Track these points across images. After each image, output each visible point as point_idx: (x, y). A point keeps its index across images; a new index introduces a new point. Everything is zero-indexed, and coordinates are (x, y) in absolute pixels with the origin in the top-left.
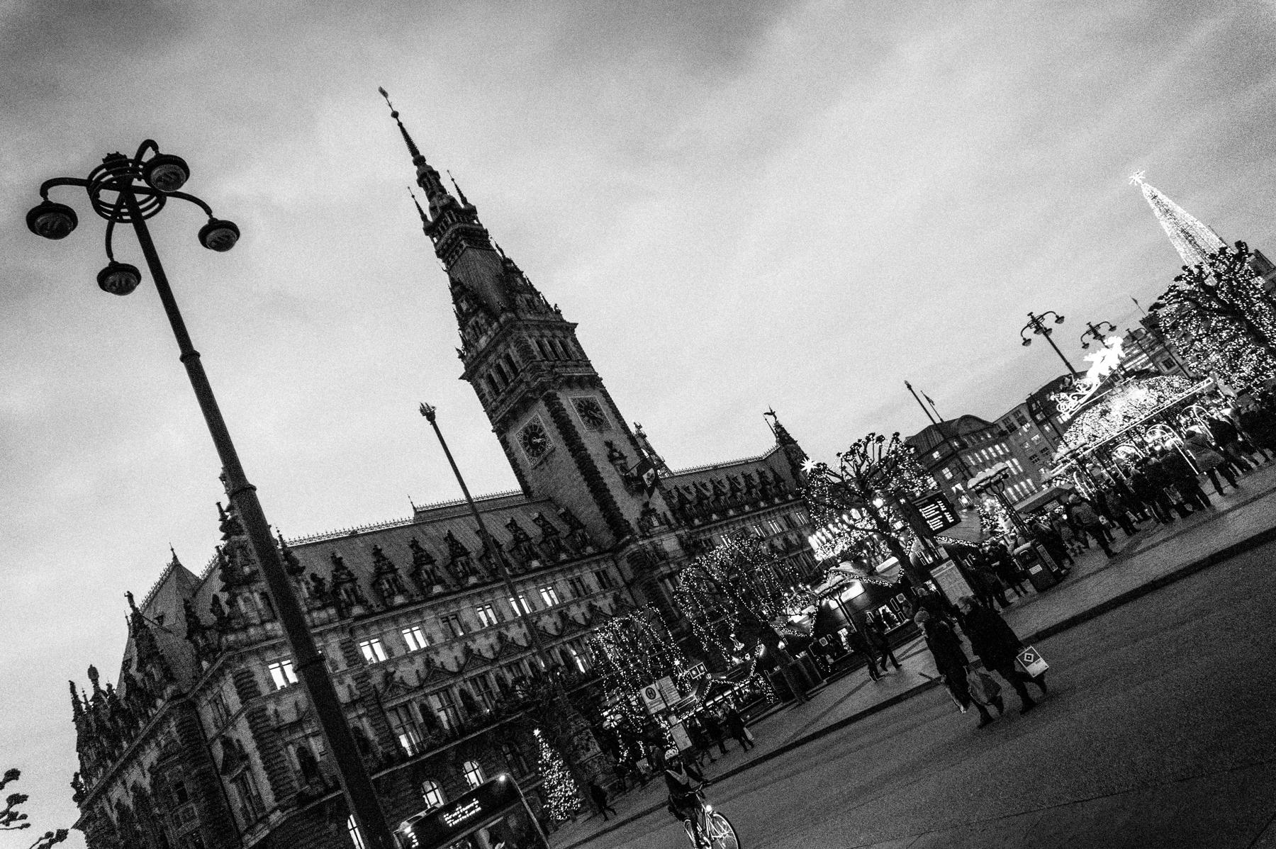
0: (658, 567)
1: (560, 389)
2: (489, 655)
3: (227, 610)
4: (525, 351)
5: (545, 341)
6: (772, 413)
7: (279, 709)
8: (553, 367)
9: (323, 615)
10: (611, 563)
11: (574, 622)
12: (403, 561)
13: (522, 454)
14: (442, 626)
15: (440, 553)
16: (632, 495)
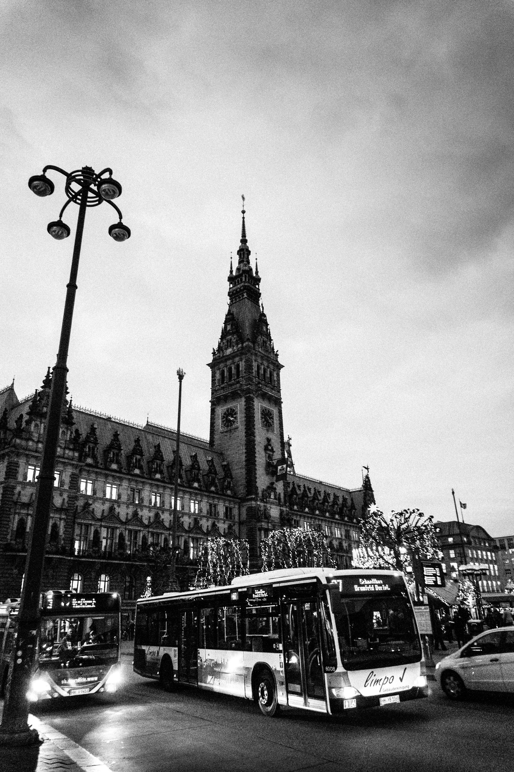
0: (262, 522)
1: (257, 397)
2: (146, 522)
3: (24, 425)
4: (249, 367)
5: (262, 367)
6: (367, 469)
7: (22, 492)
8: (259, 383)
9: (71, 454)
10: (237, 506)
11: (200, 528)
12: (127, 447)
13: (219, 422)
14: (129, 492)
15: (148, 451)
16: (267, 474)
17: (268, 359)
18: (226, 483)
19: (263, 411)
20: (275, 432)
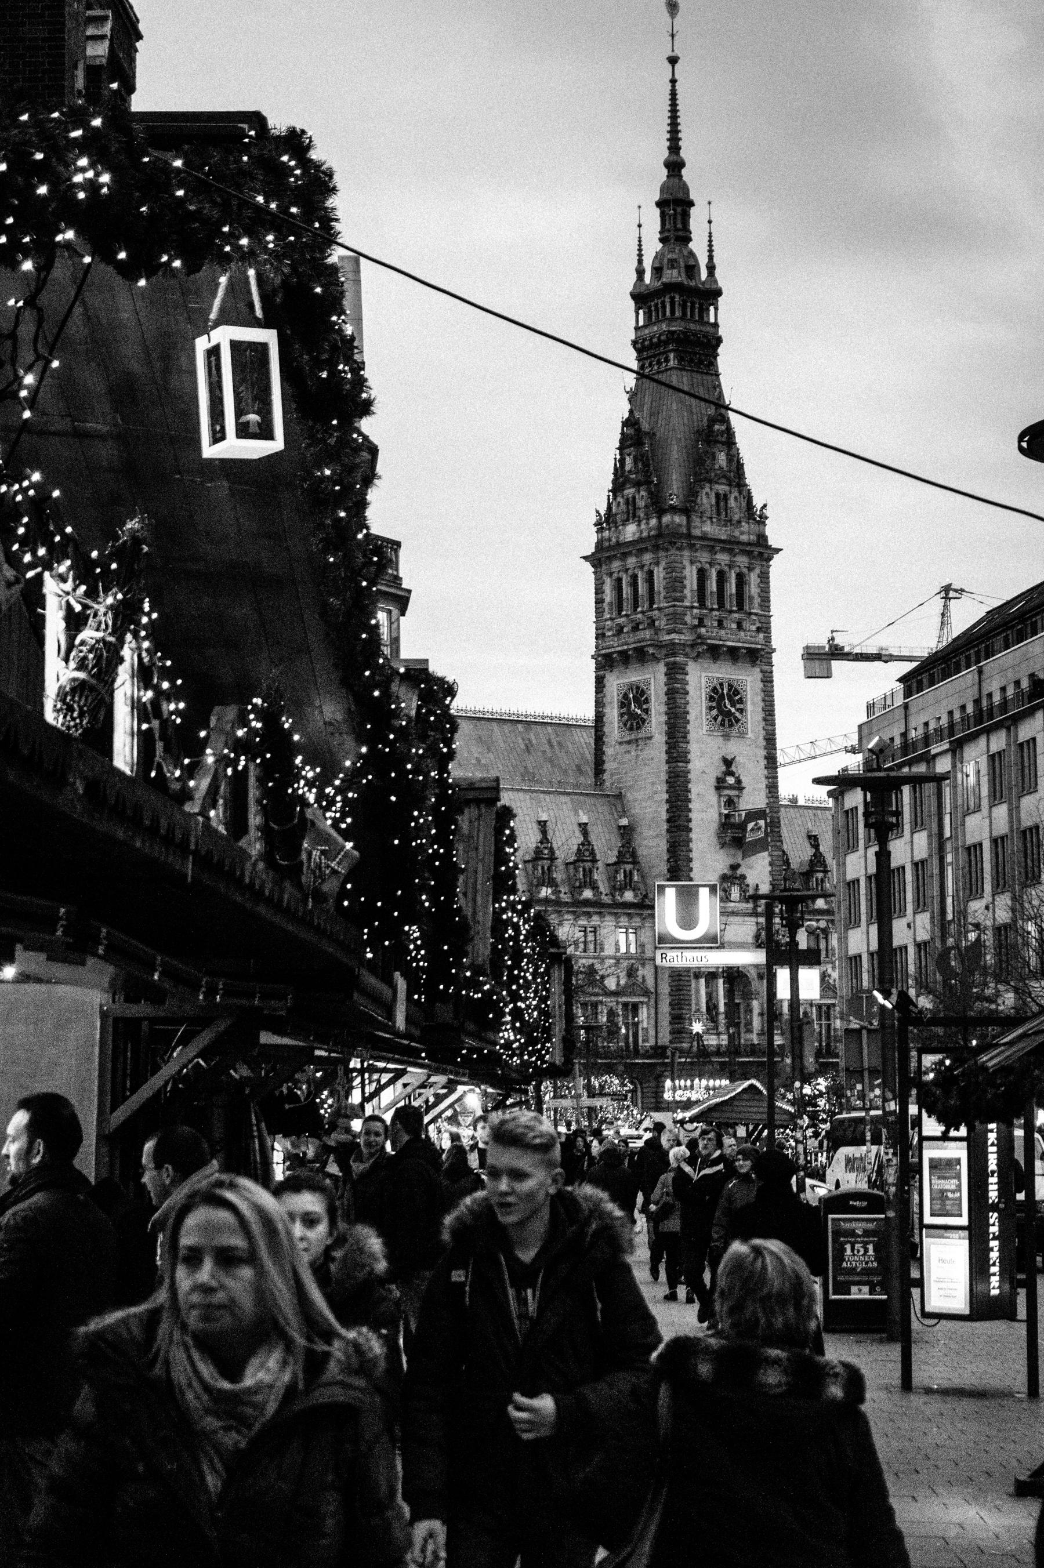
13: (613, 713)
16: (723, 845)
17: (731, 546)
18: (621, 877)
19: (714, 690)
20: (750, 735)
